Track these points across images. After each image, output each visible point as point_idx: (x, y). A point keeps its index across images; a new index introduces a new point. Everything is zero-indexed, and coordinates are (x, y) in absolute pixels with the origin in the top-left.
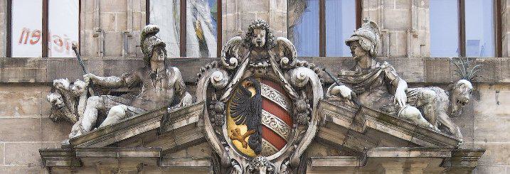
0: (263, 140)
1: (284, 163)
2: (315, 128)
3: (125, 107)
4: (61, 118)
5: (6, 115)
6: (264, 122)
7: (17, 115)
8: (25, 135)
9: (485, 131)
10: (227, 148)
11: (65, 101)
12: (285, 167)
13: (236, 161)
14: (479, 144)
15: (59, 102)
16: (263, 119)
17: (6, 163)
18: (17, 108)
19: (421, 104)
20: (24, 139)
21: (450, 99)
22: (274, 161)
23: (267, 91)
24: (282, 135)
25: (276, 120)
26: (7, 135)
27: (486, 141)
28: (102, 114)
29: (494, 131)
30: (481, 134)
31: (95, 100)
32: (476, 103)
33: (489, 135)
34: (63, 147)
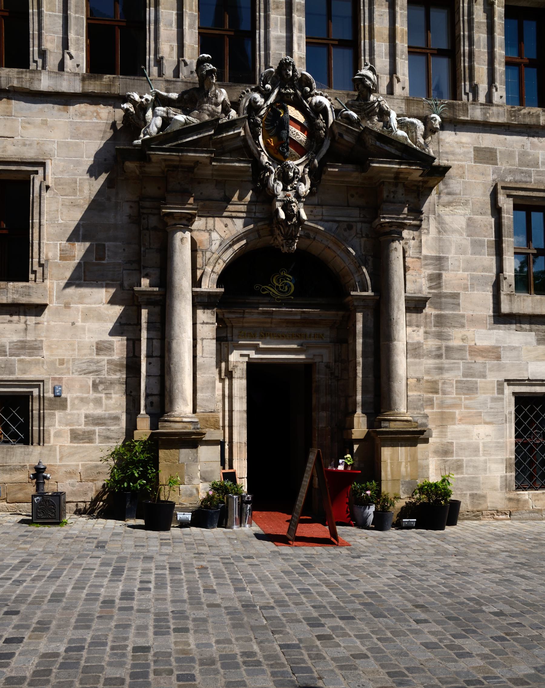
0: (290, 148)
2: (329, 142)
3: (185, 116)
4: (133, 123)
5: (86, 119)
7: (95, 120)
9: (447, 153)
10: (262, 153)
14: (444, 162)
15: (132, 110)
16: (290, 132)
18: (95, 114)
21: (425, 128)
22: (298, 165)
23: (293, 112)
27: (448, 160)
28: (167, 121)
29: (453, 154)
30: (444, 155)
31: (161, 110)
32: (441, 132)
33: (450, 157)
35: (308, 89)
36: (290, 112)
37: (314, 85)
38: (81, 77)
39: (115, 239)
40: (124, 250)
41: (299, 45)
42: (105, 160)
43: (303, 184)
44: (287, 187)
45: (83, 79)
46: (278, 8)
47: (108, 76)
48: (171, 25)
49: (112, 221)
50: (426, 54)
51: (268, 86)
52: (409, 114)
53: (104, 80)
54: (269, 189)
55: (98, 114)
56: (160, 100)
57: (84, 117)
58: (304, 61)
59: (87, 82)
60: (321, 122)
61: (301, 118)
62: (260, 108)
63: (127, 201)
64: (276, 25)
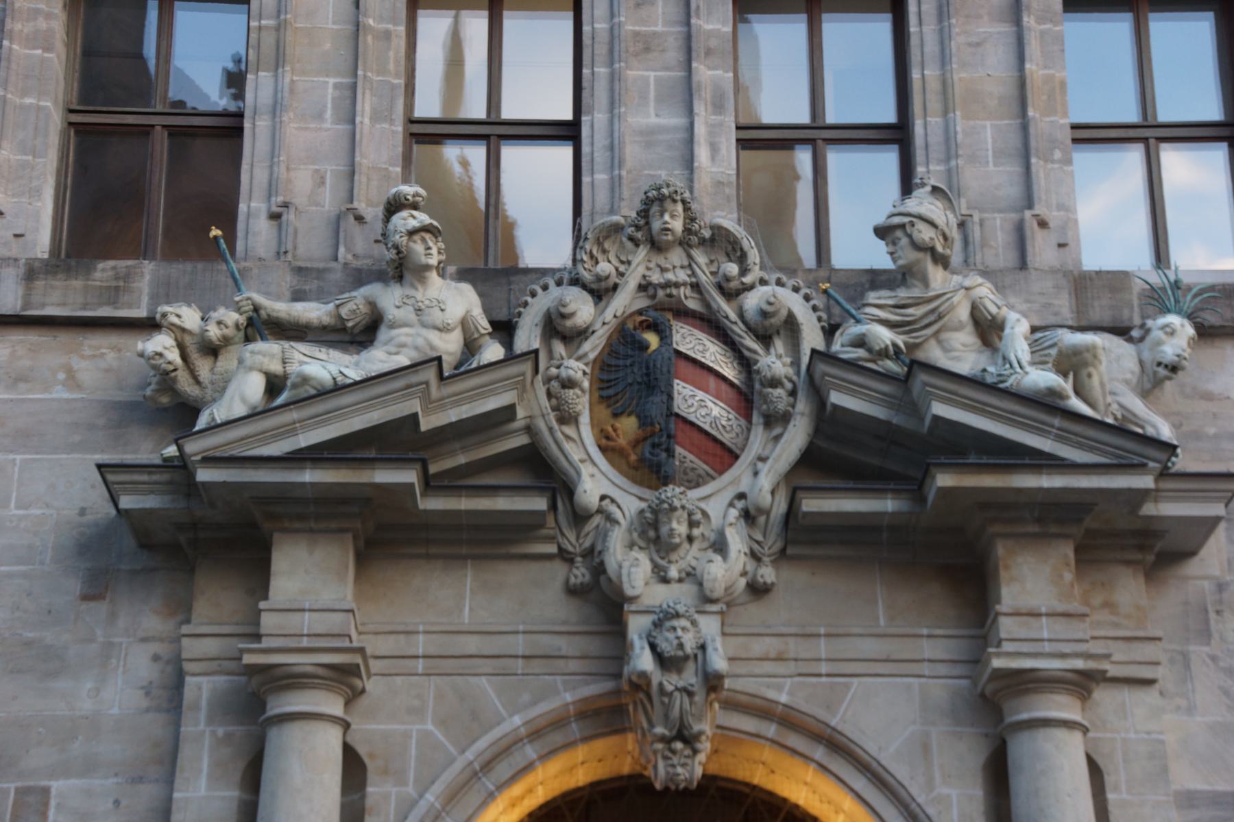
0: (679, 450)
1: (731, 505)
6: (680, 406)
7: (60, 393)
8: (77, 438)
11: (184, 356)
12: (733, 513)
13: (613, 501)
17: (18, 508)
18: (61, 376)
19: (1073, 364)
20: (72, 448)
24: (726, 438)
25: (710, 404)
26: (25, 438)
34: (167, 464)
35: (733, 269)
36: (676, 338)
37: (754, 256)
38: (22, 271)
39: (89, 767)
40: (117, 803)
41: (714, 149)
42: (82, 512)
43: (718, 558)
44: (665, 570)
45: (31, 273)
46: (647, 49)
47: (111, 263)
48: (320, 116)
49: (86, 706)
50: (1145, 140)
51: (604, 267)
52: (1084, 323)
53: (98, 275)
54: (610, 580)
55: (70, 373)
56: (260, 326)
57: (22, 386)
58: (731, 191)
59: (40, 284)
60: (775, 362)
61: (712, 353)
62: (583, 334)
63: (144, 640)
64: (644, 97)
